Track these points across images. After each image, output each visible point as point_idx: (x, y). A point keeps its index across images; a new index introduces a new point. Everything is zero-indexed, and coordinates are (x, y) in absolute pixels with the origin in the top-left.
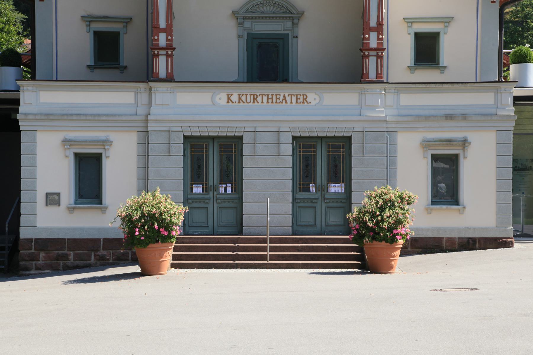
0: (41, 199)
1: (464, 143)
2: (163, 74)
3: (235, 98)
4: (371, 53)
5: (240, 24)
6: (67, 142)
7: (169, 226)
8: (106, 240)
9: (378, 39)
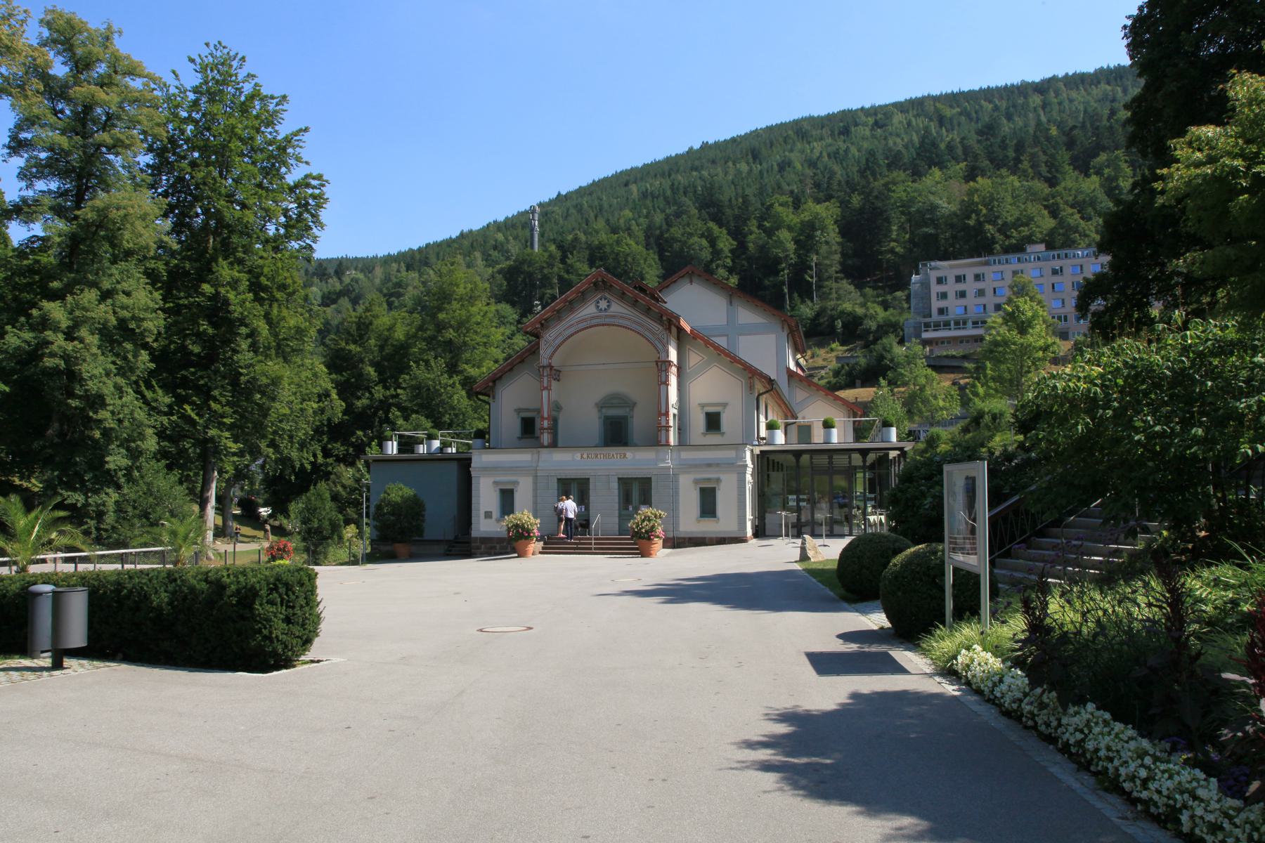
0: (482, 515)
1: (718, 480)
2: (546, 443)
6: (496, 483)
7: (529, 531)
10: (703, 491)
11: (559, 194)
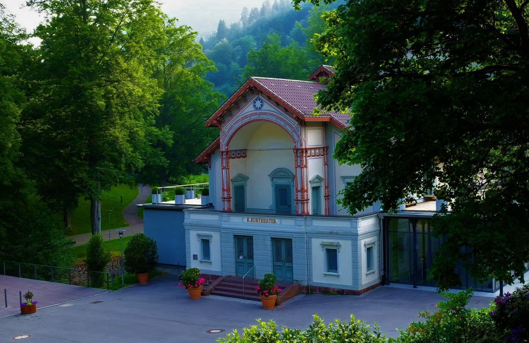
3: (250, 220)
5: (272, 180)
10: (328, 250)
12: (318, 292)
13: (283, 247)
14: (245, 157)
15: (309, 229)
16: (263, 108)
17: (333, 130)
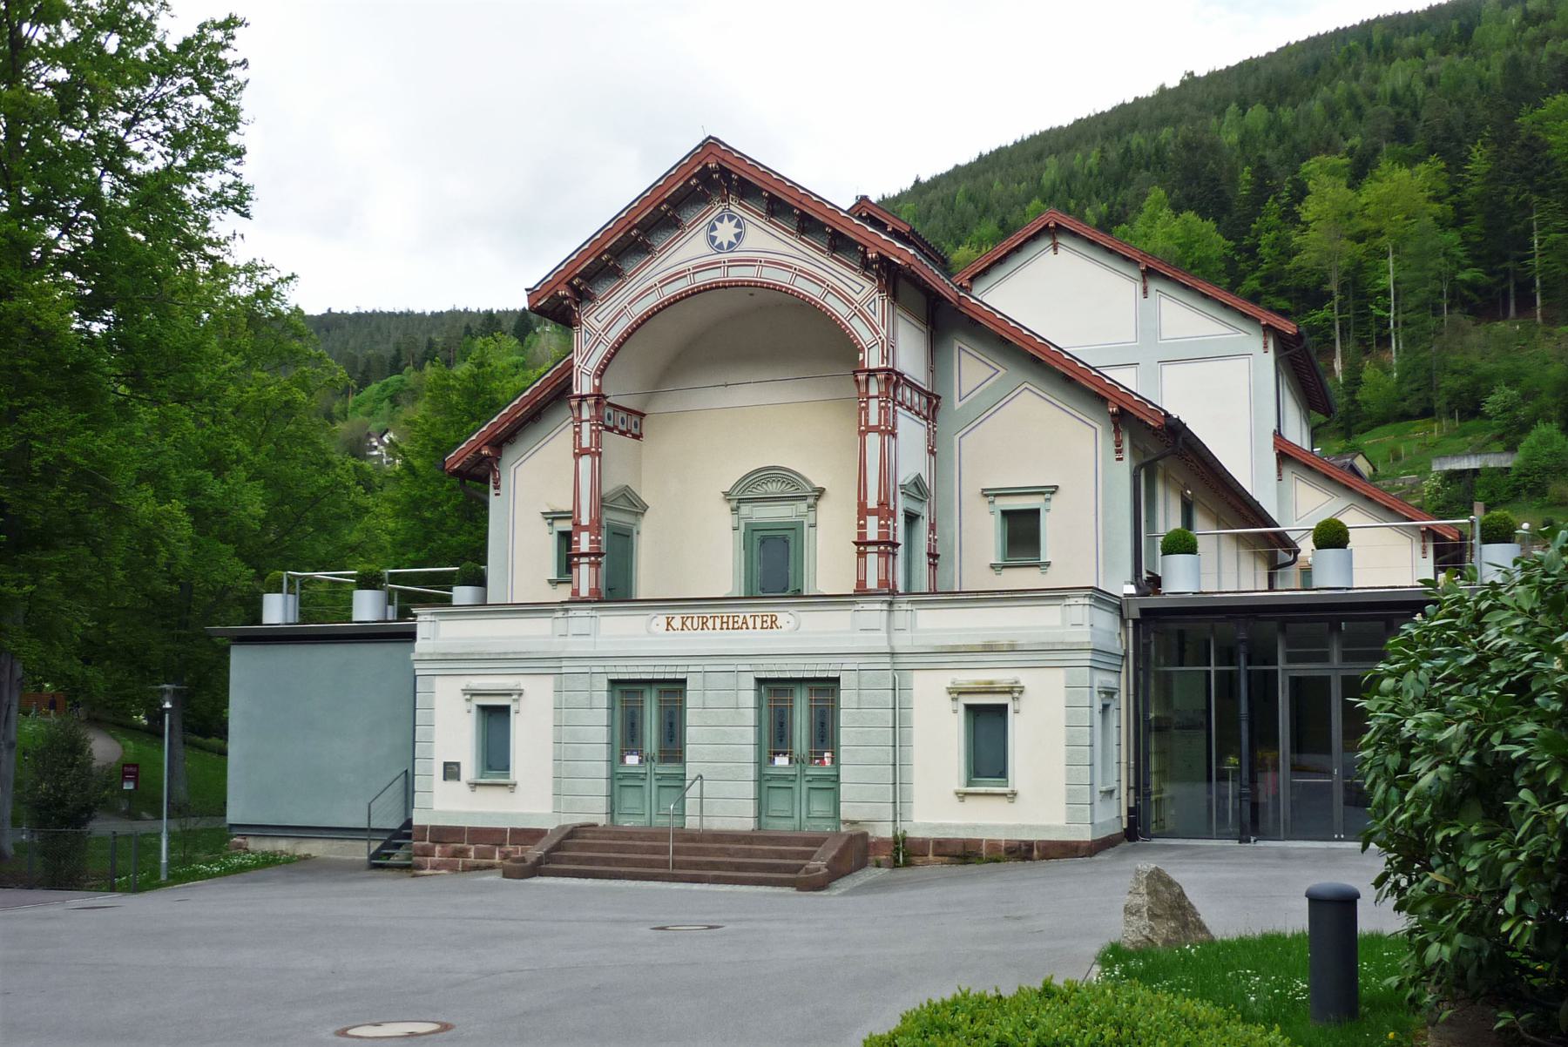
3: (677, 623)
4: (869, 549)
5: (735, 510)
8: (514, 831)
9: (880, 526)
11: (917, 182)
12: (931, 857)
13: (800, 712)
14: (637, 437)
15: (902, 642)
16: (746, 243)
17: (957, 344)
